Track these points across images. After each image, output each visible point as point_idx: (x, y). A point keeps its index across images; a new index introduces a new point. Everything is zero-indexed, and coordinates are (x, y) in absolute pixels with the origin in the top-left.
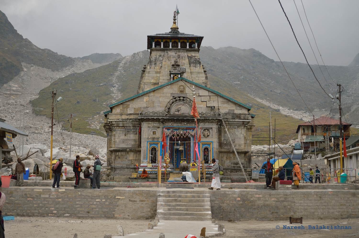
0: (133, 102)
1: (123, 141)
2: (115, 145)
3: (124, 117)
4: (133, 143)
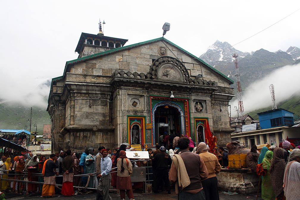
0: (102, 61)
1: (88, 116)
2: (74, 121)
3: (88, 80)
4: (101, 118)
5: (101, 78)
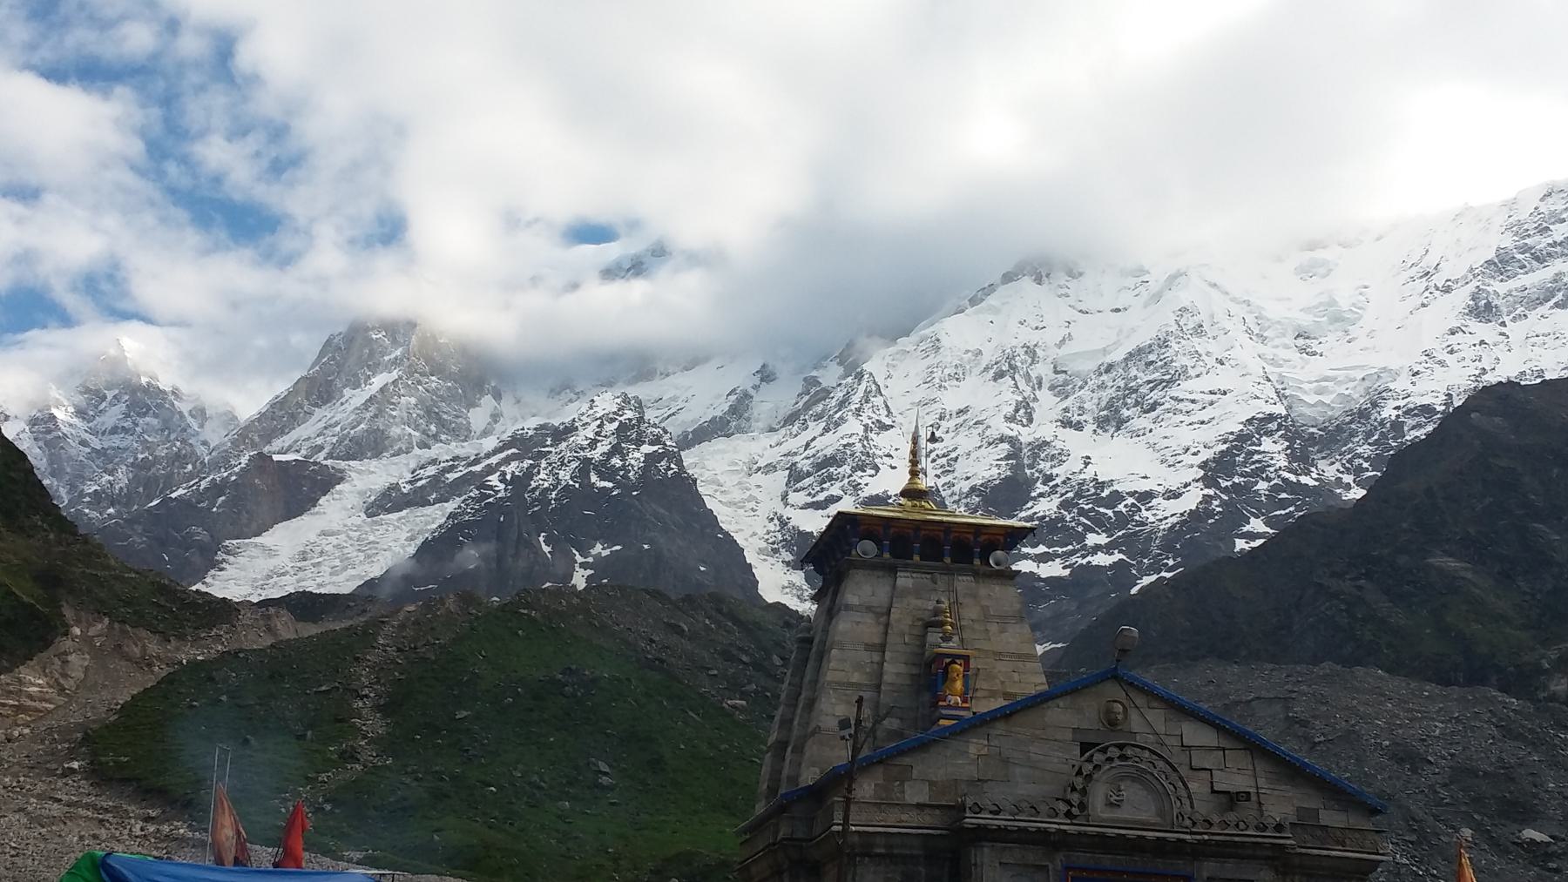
5: (927, 811)
